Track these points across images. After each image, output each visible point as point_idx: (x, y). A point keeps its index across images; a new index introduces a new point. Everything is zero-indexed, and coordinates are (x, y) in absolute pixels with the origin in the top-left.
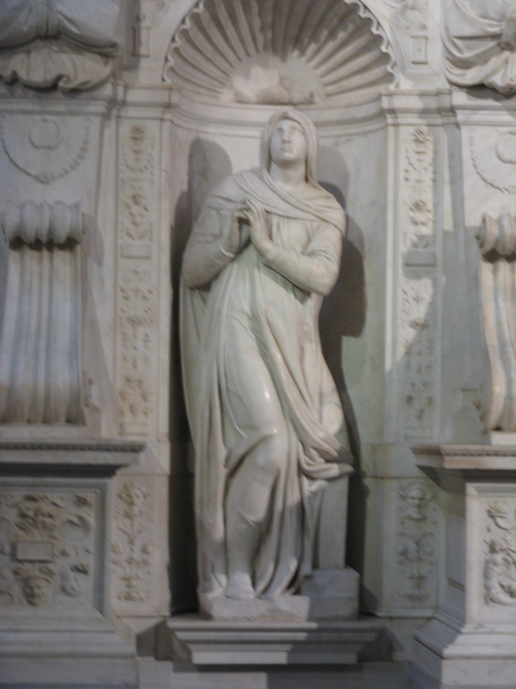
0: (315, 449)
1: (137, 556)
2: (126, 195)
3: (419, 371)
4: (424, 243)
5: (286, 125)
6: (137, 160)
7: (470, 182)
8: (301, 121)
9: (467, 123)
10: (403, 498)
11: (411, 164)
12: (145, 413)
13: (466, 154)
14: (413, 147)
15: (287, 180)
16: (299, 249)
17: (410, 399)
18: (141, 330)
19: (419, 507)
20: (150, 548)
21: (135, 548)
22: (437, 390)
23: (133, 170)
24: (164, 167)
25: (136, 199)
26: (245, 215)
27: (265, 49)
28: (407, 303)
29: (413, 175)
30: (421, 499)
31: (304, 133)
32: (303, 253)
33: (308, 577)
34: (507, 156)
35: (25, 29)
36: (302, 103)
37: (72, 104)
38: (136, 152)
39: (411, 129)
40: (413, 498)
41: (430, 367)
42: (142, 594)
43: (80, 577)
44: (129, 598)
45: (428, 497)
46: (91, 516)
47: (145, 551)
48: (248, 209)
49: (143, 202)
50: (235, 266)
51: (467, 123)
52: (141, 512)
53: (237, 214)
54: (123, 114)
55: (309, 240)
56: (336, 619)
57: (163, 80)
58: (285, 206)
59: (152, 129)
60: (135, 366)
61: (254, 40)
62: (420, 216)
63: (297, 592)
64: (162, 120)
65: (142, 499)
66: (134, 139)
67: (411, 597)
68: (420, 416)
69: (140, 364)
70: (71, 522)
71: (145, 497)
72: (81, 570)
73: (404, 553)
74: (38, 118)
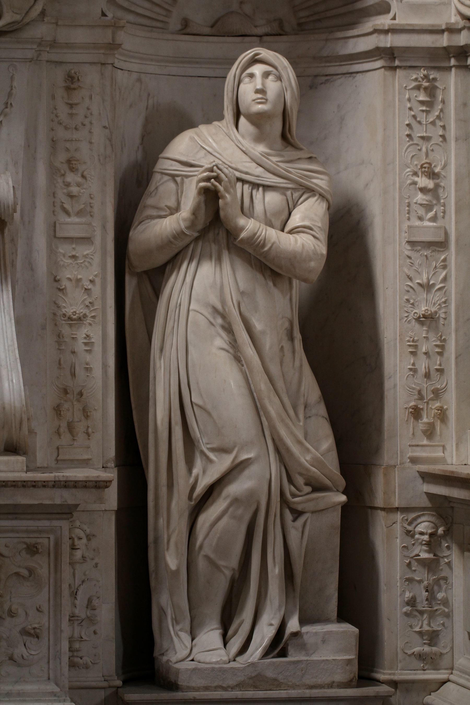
0: (300, 474)
1: (81, 612)
3: (427, 376)
5: (258, 69)
6: (71, 115)
8: (277, 64)
10: (409, 534)
11: (414, 117)
12: (88, 434)
16: (278, 223)
17: (416, 413)
19: (428, 544)
20: (95, 602)
21: (77, 602)
22: (451, 401)
23: (66, 128)
25: (71, 164)
26: (213, 184)
28: (411, 290)
30: (431, 535)
32: (283, 230)
33: (295, 635)
38: (71, 106)
40: (422, 533)
41: (441, 371)
42: (87, 659)
43: (31, 641)
45: (441, 531)
46: (42, 566)
48: (217, 178)
49: (81, 168)
52: (83, 557)
53: (202, 184)
55: (290, 214)
56: (331, 685)
57: (104, 15)
59: (91, 77)
60: (73, 375)
63: (283, 654)
65: (84, 541)
66: (68, 89)
67: (421, 657)
68: (430, 433)
69: (80, 371)
70: (17, 574)
71: (89, 539)
72: (32, 634)
73: (412, 602)
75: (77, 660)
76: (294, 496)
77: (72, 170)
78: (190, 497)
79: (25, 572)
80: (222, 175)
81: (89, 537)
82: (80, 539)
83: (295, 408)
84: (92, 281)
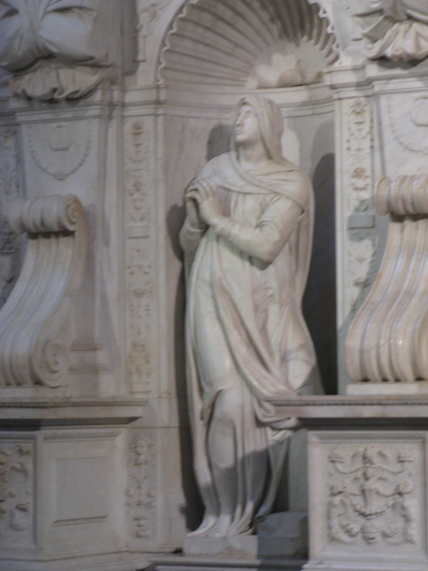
1: (144, 499)
2: (129, 185)
4: (364, 207)
7: (391, 146)
9: (383, 93)
13: (385, 121)
14: (353, 118)
15: (248, 159)
18: (144, 301)
24: (160, 156)
25: (137, 186)
27: (281, 37)
29: (354, 145)
31: (256, 115)
34: (420, 121)
35: (20, 54)
36: (313, 83)
37: (69, 112)
39: (352, 102)
43: (22, 514)
44: (139, 536)
47: (149, 495)
50: (204, 240)
51: (383, 93)
54: (126, 114)
56: (282, 557)
58: (241, 183)
59: (148, 124)
60: (139, 333)
61: (269, 30)
62: (360, 183)
63: (254, 533)
64: (157, 115)
74: (55, 125)
75: (141, 533)
76: (265, 416)
77: (138, 190)
78: (202, 418)
79: (18, 466)
80: (200, 188)
81: (150, 446)
82: (143, 447)
83: (271, 354)
84: (150, 267)
